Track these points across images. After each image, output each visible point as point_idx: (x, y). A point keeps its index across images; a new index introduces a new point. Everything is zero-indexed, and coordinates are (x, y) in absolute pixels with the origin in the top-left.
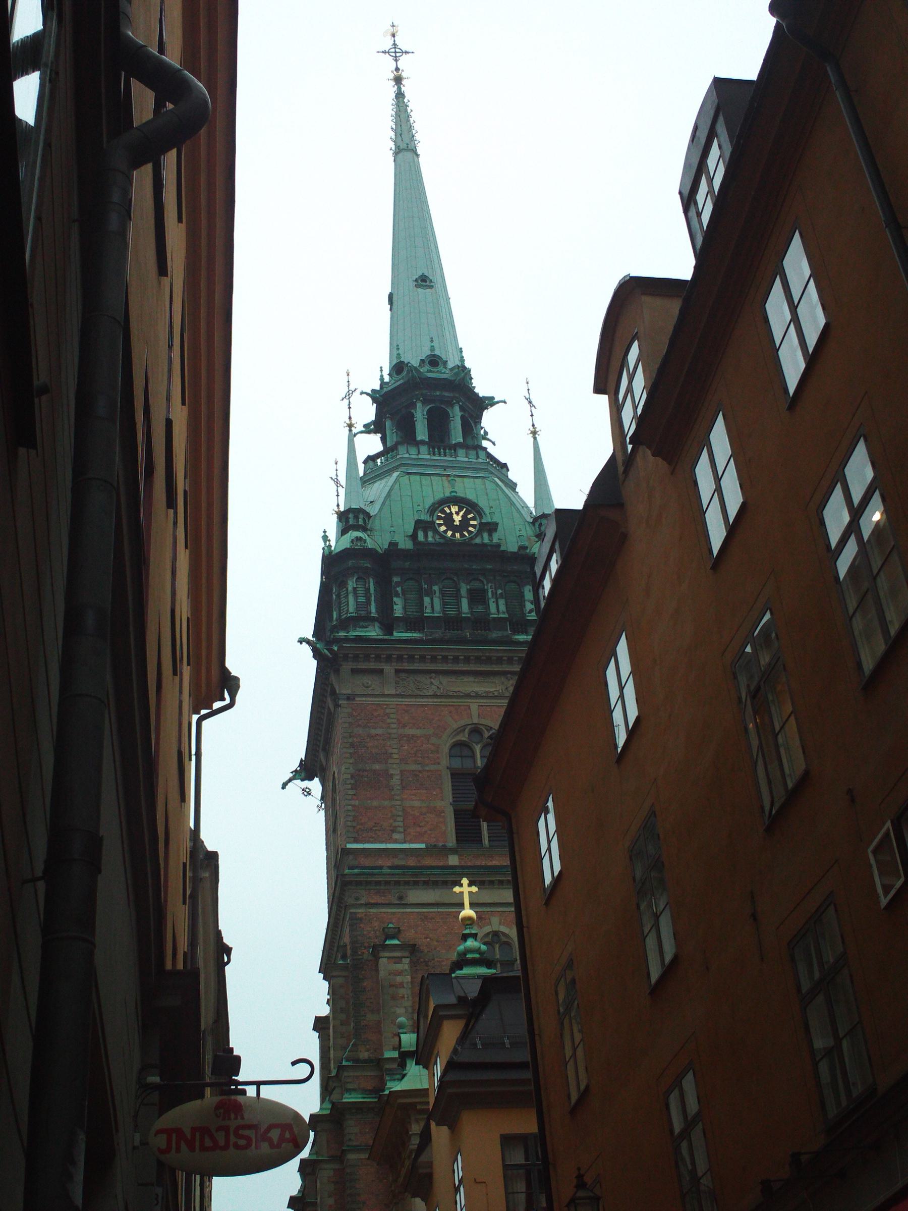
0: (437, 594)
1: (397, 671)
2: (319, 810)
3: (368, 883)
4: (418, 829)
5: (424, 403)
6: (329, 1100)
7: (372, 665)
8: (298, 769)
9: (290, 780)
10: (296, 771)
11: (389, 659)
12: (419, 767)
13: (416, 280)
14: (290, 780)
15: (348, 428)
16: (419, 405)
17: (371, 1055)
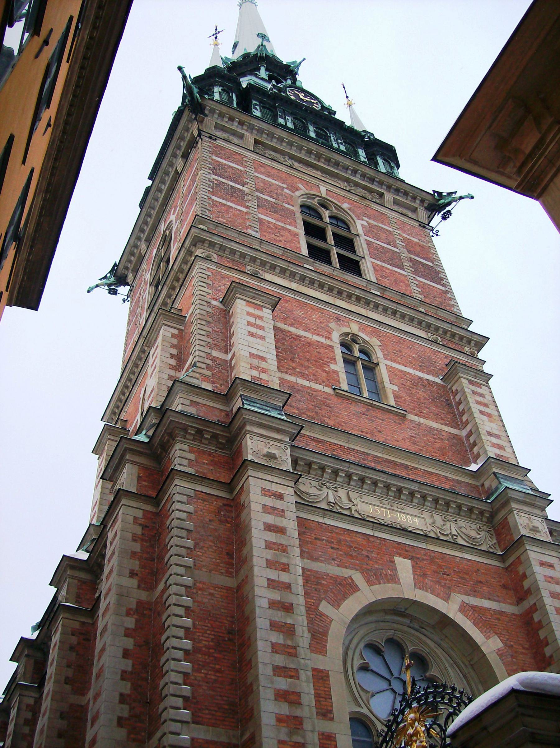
0: (290, 120)
1: (257, 142)
2: (124, 302)
3: (222, 248)
4: (274, 236)
5: (267, 70)
6: (145, 434)
7: (234, 126)
8: (109, 275)
9: (97, 286)
10: (105, 277)
11: (251, 128)
13: (258, 35)
14: (97, 286)
15: (213, 47)
16: (263, 69)
17: (215, 389)
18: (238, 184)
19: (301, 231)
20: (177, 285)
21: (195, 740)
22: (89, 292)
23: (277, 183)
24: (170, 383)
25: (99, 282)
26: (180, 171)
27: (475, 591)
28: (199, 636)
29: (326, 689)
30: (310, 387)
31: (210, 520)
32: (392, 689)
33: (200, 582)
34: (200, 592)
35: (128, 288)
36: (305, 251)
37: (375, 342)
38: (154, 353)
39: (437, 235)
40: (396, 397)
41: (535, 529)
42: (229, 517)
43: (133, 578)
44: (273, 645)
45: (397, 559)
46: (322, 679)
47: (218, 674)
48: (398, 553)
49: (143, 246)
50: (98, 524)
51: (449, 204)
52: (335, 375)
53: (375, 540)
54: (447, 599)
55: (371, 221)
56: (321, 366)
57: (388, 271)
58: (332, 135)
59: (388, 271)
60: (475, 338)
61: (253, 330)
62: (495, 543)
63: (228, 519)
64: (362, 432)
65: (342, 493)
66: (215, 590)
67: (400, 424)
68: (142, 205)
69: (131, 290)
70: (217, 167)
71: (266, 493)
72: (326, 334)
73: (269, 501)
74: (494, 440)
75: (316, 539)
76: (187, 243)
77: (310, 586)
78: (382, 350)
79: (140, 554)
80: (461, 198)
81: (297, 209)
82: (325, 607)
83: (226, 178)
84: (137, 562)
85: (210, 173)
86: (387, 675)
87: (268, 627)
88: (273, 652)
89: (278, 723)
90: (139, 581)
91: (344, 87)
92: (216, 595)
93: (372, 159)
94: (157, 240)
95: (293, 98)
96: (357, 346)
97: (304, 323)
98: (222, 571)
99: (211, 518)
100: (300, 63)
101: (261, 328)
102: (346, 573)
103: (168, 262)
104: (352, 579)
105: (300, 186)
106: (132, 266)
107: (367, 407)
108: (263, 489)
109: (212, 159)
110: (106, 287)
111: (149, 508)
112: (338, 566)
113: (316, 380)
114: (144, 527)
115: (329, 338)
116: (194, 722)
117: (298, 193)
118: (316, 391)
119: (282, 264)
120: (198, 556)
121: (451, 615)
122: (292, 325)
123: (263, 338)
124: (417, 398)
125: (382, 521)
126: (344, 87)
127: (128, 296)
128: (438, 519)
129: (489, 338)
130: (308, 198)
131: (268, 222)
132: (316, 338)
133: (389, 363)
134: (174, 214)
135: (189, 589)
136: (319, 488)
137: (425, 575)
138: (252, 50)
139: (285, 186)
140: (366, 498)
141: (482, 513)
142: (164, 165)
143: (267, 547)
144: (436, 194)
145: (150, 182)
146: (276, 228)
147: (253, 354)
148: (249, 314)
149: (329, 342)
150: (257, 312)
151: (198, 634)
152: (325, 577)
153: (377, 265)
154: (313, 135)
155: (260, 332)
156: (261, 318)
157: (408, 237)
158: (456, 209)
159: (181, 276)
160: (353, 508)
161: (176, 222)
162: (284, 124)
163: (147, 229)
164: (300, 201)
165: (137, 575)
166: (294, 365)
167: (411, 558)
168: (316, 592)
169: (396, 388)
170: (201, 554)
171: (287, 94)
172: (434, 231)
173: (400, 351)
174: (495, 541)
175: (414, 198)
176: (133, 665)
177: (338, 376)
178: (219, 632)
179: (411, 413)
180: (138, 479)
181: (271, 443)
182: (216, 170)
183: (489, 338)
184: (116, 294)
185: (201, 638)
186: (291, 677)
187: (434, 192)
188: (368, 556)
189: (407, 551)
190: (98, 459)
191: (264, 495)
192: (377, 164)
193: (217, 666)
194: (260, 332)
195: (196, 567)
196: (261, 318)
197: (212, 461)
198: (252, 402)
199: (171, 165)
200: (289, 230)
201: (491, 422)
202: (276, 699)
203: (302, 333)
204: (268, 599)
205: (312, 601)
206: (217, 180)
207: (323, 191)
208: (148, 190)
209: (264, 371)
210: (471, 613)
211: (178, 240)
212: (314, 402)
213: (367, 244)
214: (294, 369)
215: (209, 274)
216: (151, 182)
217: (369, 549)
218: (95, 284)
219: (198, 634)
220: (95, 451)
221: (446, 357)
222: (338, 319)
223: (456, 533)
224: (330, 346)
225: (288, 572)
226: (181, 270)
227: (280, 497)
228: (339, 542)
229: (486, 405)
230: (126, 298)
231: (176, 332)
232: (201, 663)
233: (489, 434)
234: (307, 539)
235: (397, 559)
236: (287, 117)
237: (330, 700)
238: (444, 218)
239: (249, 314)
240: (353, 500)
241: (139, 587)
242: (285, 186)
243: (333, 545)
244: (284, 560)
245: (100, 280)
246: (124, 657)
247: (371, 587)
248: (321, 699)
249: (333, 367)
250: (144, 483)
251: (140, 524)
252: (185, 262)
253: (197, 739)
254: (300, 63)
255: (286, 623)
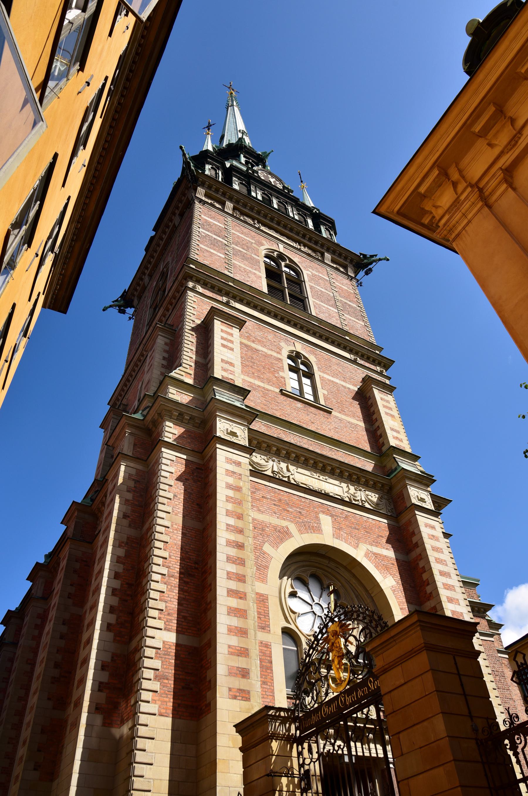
0: (260, 195)
1: (234, 209)
4: (243, 277)
5: (244, 157)
6: (141, 414)
8: (119, 299)
9: (111, 306)
10: (117, 301)
12: (245, 251)
14: (111, 306)
16: (242, 156)
18: (219, 237)
19: (263, 274)
20: (170, 307)
21: (166, 643)
22: (104, 310)
23: (248, 239)
24: (161, 378)
25: (112, 303)
26: (177, 225)
27: (377, 543)
28: (173, 564)
29: (265, 609)
30: (264, 388)
31: (186, 479)
32: (313, 612)
33: (176, 524)
34: (175, 532)
35: (133, 309)
36: (265, 290)
37: (312, 359)
38: (151, 356)
39: (361, 286)
40: (326, 399)
41: (422, 500)
42: (200, 478)
43: (125, 519)
44: (228, 573)
45: (322, 516)
46: (263, 601)
47: (185, 594)
48: (322, 511)
49: (146, 279)
50: (101, 480)
51: (371, 263)
52: (283, 380)
53: (306, 501)
54: (356, 547)
55: (314, 272)
56: (273, 373)
57: (324, 309)
58: (289, 208)
59: (324, 309)
60: (384, 361)
61: (225, 343)
62: (392, 509)
63: (199, 479)
64: (300, 422)
65: (283, 465)
66: (186, 530)
67: (328, 418)
68: (147, 249)
69: (135, 311)
70: (205, 224)
71: (229, 461)
72: (278, 350)
73: (231, 467)
74: (395, 434)
75: (263, 497)
76: (180, 277)
77: (257, 531)
78: (317, 364)
79: (132, 502)
80: (380, 260)
81: (262, 259)
82: (267, 548)
83: (211, 232)
84: (130, 508)
85: (200, 228)
86: (310, 602)
87: (225, 560)
88: (227, 578)
89: (229, 632)
90: (130, 521)
91: (300, 174)
92: (187, 535)
93: (317, 226)
94: (157, 276)
95: (263, 178)
96: (299, 361)
97: (262, 341)
98: (193, 517)
99: (187, 478)
100: (269, 154)
101: (232, 342)
102: (284, 523)
103: (164, 291)
104: (288, 528)
105: (264, 242)
106: (137, 293)
107: (304, 405)
108: (227, 458)
109: (202, 218)
110: (117, 308)
111: (140, 467)
112: (278, 518)
113: (269, 381)
114: (136, 481)
115: (279, 353)
116: (165, 629)
117: (262, 248)
118: (268, 390)
119: (248, 298)
120: (176, 504)
121: (359, 559)
122: (253, 342)
123: (232, 349)
124: (341, 401)
125: (311, 487)
126: (300, 174)
127: (133, 315)
128: (352, 489)
129: (394, 362)
130: (269, 252)
131: (240, 266)
132: (270, 352)
133: (322, 374)
134: (171, 256)
135: (167, 529)
136: (267, 460)
137: (340, 529)
138: (234, 141)
139: (254, 242)
140: (300, 470)
141: (383, 485)
142: (166, 220)
143: (227, 501)
144: (362, 256)
145: (154, 233)
146: (245, 271)
147: (224, 360)
148: (222, 331)
149: (279, 356)
150: (229, 330)
151: (172, 562)
152: (268, 525)
153: (317, 304)
154: (276, 206)
155: (230, 345)
156: (232, 335)
157: (340, 285)
158: (376, 268)
159: (174, 301)
160: (291, 477)
161: (172, 262)
162: (255, 196)
163: (150, 267)
164: (264, 252)
165: (129, 517)
166: (253, 371)
167: (332, 516)
168: (261, 536)
169: (326, 393)
170: (178, 503)
171: (258, 175)
172: (359, 283)
173: (330, 367)
174: (393, 507)
175: (346, 258)
176: (122, 585)
177: (285, 381)
178: (188, 562)
179: (335, 411)
180: (134, 446)
181: (234, 425)
182: (204, 226)
183: (394, 362)
184: (124, 314)
185: (174, 566)
186: (241, 598)
187: (361, 254)
188: (300, 512)
189: (328, 510)
190: (104, 432)
191: (228, 462)
192: (320, 232)
193: (185, 588)
194: (230, 345)
195: (173, 513)
196: (232, 335)
197: (189, 436)
198: (222, 394)
199: (171, 220)
200: (255, 274)
201: (393, 420)
202: (228, 615)
203: (259, 347)
204: (226, 539)
205: (258, 543)
206: (204, 233)
207: (281, 248)
208: (152, 238)
209: (232, 373)
210: (373, 558)
211: (173, 275)
212: (266, 398)
213: (310, 288)
214: (253, 373)
215: (196, 300)
216: (155, 233)
217: (302, 507)
218: (108, 305)
219: (172, 562)
220: (102, 426)
221: (363, 373)
222: (286, 341)
223: (365, 500)
224: (280, 359)
225: (242, 520)
226: (174, 297)
227: (239, 464)
228: (280, 500)
229: (390, 409)
230: (131, 316)
231: (168, 341)
232: (173, 585)
233: (392, 429)
234: (257, 497)
235: (322, 516)
236: (257, 192)
237: (268, 617)
238: (367, 273)
239: (222, 331)
240: (291, 471)
241: (130, 526)
242: (254, 242)
243: (275, 503)
244: (239, 511)
245: (113, 302)
246: (115, 578)
247: (302, 535)
248: (261, 616)
249: (281, 374)
250: (138, 449)
251: (133, 480)
252: (177, 290)
253: (167, 642)
254: (269, 154)
255: (238, 558)
